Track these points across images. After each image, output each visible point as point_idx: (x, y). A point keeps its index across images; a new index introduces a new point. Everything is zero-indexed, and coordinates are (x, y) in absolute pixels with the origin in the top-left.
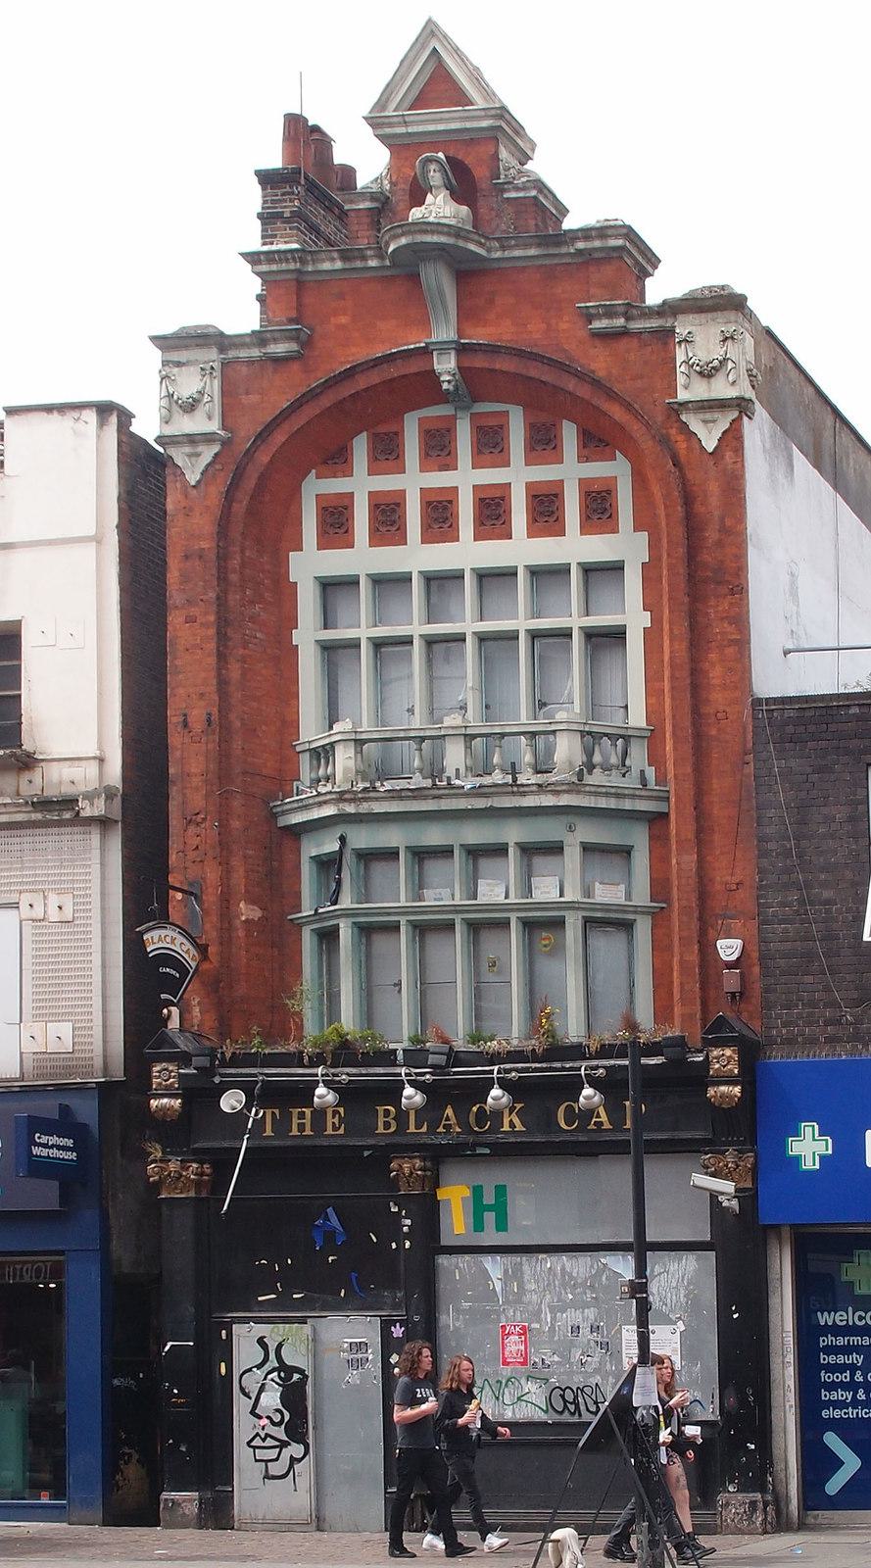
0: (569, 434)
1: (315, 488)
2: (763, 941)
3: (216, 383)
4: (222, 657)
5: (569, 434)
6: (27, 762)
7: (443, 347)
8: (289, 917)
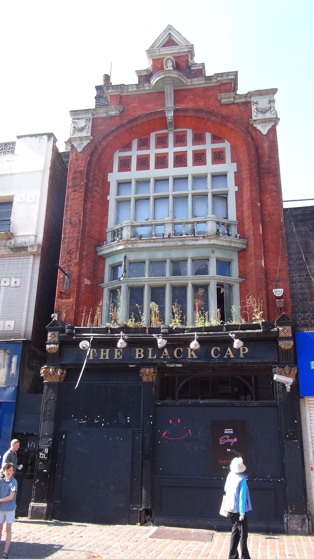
0: (208, 136)
1: (118, 155)
2: (292, 289)
3: (91, 123)
4: (85, 201)
5: (208, 136)
8: (99, 285)
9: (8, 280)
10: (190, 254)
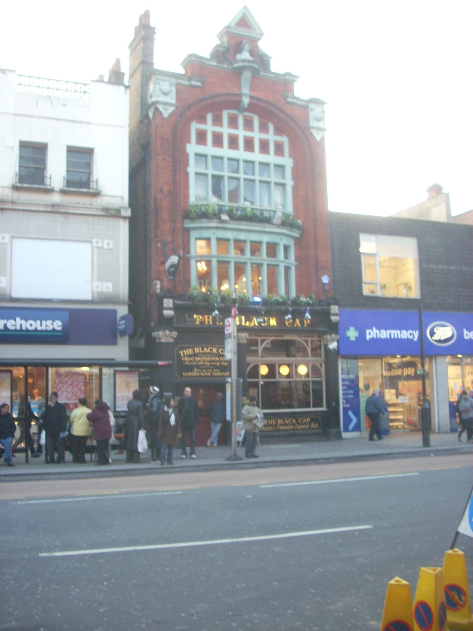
0: (271, 127)
5: (271, 127)
6: (96, 194)
7: (246, 95)
9: (100, 241)
10: (265, 239)
